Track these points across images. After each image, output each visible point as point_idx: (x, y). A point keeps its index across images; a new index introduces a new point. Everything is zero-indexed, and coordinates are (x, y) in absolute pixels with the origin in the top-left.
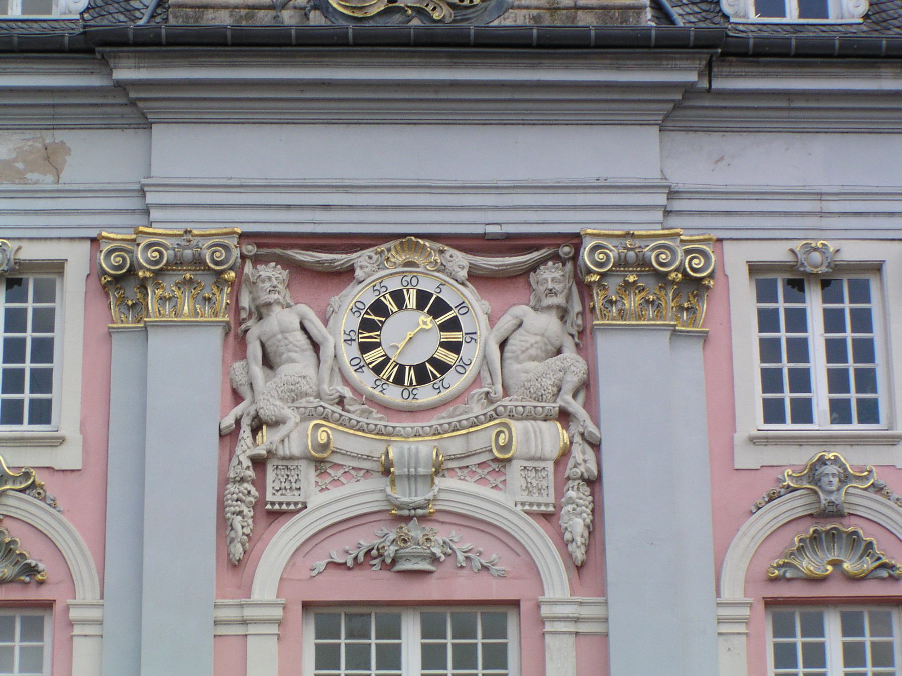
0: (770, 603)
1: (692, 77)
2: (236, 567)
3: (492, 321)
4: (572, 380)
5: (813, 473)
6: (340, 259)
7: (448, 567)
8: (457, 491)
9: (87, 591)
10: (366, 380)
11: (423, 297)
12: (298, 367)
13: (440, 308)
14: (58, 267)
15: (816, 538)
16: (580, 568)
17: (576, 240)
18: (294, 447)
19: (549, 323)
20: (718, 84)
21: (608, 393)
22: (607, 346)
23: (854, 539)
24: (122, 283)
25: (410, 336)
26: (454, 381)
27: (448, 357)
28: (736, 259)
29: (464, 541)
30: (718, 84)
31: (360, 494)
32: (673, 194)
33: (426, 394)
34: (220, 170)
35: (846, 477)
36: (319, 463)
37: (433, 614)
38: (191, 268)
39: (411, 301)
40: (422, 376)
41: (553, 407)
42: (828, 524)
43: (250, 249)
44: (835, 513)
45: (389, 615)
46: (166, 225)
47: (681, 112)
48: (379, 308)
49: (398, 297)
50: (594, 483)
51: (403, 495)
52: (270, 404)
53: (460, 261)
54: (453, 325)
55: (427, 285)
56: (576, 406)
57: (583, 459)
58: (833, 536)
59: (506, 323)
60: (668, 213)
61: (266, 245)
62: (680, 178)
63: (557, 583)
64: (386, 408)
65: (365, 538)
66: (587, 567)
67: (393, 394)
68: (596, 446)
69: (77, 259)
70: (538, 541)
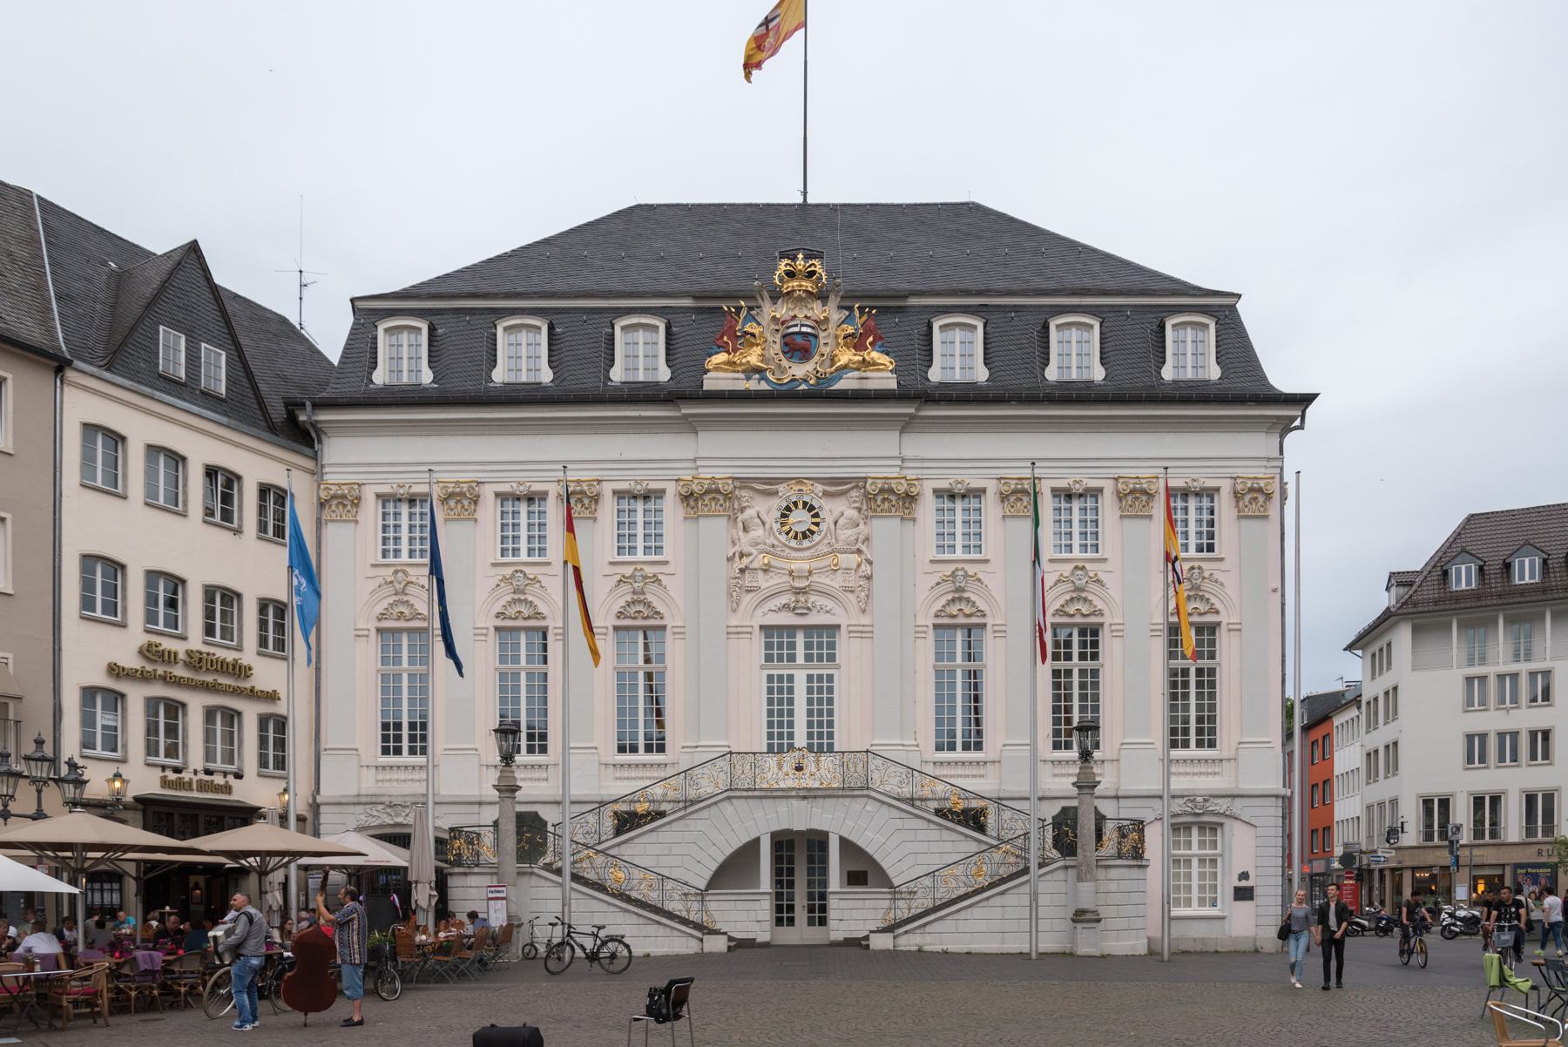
0: (936, 626)
4: (862, 537)
7: (814, 612)
10: (783, 538)
11: (805, 504)
12: (757, 533)
13: (812, 508)
14: (663, 491)
15: (953, 600)
16: (864, 611)
18: (755, 565)
20: (923, 413)
21: (875, 541)
23: (968, 600)
24: (688, 498)
25: (800, 519)
26: (816, 538)
27: (814, 528)
28: (927, 488)
30: (923, 413)
32: (903, 460)
33: (806, 543)
34: (723, 452)
35: (966, 575)
36: (765, 571)
37: (809, 629)
38: (713, 492)
40: (805, 536)
41: (854, 548)
42: (959, 595)
43: (737, 484)
44: (960, 590)
45: (791, 630)
46: (706, 473)
48: (788, 508)
49: (795, 504)
50: (869, 578)
51: (798, 584)
53: (819, 488)
54: (816, 515)
55: (807, 499)
56: (863, 548)
57: (865, 568)
58: (960, 599)
60: (901, 468)
61: (745, 483)
62: (907, 453)
65: (784, 599)
67: (793, 543)
69: (671, 489)
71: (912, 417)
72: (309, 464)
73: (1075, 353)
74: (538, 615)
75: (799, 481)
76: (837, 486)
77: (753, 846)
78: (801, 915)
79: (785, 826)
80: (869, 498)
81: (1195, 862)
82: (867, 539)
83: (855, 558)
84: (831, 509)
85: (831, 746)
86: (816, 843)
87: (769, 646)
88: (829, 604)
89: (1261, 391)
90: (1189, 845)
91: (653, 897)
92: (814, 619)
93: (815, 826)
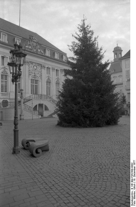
1: (46, 58)
2: (29, 77)
5: (48, 76)
8: (37, 75)
9: (23, 77)
17: (41, 64)
19: (40, 68)
22: (42, 69)
25: (35, 67)
29: (36, 77)
31: (33, 74)
42: (49, 79)
47: (45, 59)
50: (42, 75)
52: (30, 70)
63: (40, 79)
65: (33, 76)
68: (42, 74)
70: (39, 77)
71: (46, 59)
73: (57, 56)
74: (7, 74)
75: (35, 63)
76: (39, 64)
77: (36, 106)
79: (40, 103)
80: (41, 66)
82: (41, 71)
83: (40, 73)
84: (38, 67)
85: (37, 94)
88: (38, 78)
92: (36, 79)
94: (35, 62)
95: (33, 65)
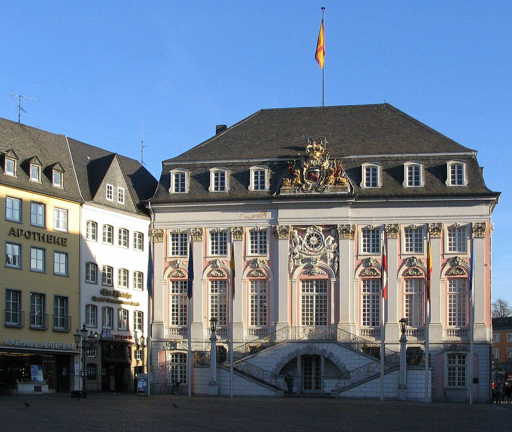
3: (325, 238)
6: (305, 229)
10: (308, 247)
17: (337, 225)
25: (314, 240)
27: (318, 243)
39: (314, 235)
40: (316, 246)
43: (292, 228)
48: (310, 236)
49: (312, 234)
50: (338, 262)
59: (327, 238)
64: (310, 251)
66: (337, 275)
67: (311, 249)
72: (149, 222)
78: (313, 385)
81: (457, 369)
86: (317, 358)
87: (303, 286)
89: (484, 191)
90: (454, 362)
91: (260, 377)
93: (316, 353)
94: (314, 223)
95: (307, 234)
